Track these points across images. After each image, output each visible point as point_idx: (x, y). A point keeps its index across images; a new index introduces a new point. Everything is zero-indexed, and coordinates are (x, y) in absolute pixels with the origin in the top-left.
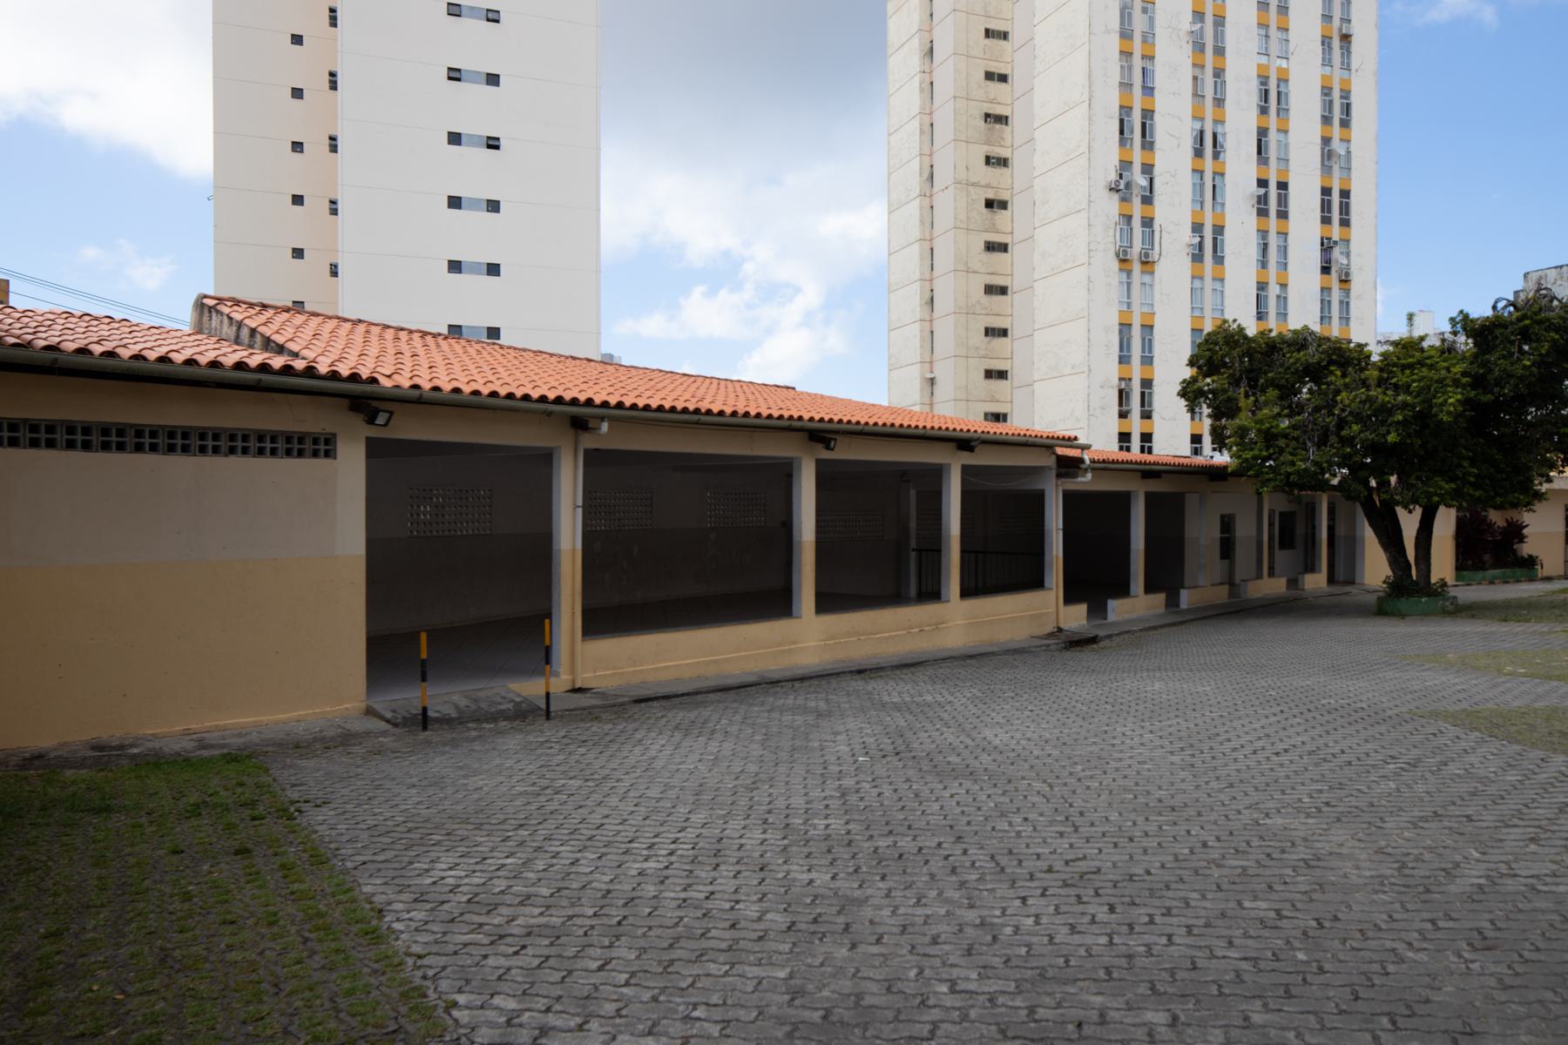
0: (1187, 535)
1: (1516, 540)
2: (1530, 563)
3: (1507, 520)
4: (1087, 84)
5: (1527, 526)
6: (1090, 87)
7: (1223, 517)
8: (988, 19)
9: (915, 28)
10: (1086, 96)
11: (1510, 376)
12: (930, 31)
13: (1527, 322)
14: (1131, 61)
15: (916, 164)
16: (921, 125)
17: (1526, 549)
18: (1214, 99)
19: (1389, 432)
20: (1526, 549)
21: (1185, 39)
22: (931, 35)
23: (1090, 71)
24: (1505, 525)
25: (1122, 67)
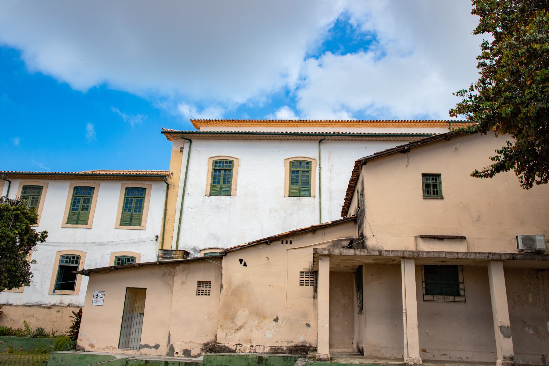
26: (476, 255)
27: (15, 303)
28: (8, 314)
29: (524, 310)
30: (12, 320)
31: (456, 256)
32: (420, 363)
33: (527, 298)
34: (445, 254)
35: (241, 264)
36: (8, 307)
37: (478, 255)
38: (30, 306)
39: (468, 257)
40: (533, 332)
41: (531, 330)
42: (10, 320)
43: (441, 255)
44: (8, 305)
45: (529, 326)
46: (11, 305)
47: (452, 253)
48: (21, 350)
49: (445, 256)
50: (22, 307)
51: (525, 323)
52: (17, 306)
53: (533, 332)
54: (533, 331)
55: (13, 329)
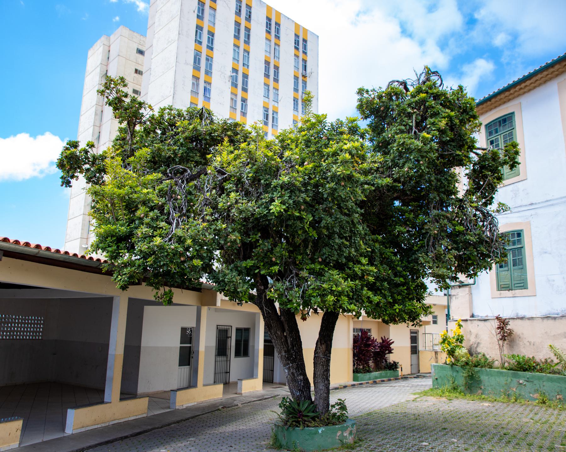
0: (143, 344)
1: (387, 352)
2: (394, 366)
3: (382, 338)
4: (173, 86)
5: (393, 342)
6: (174, 88)
7: (184, 330)
8: (137, 65)
9: (99, 62)
10: (172, 93)
11: (409, 150)
12: (107, 66)
13: (423, 95)
14: (198, 82)
15: (91, 130)
16: (96, 111)
17: (391, 358)
18: (241, 111)
19: (272, 200)
20: (391, 358)
21: (227, 79)
22: (107, 68)
23: (175, 80)
24: (381, 341)
25: (193, 84)
27: (528, 315)
28: (523, 334)
30: (532, 344)
36: (519, 322)
38: (555, 318)
42: (528, 344)
44: (518, 318)
46: (522, 318)
48: (559, 399)
50: (540, 320)
52: (531, 318)
55: (537, 359)
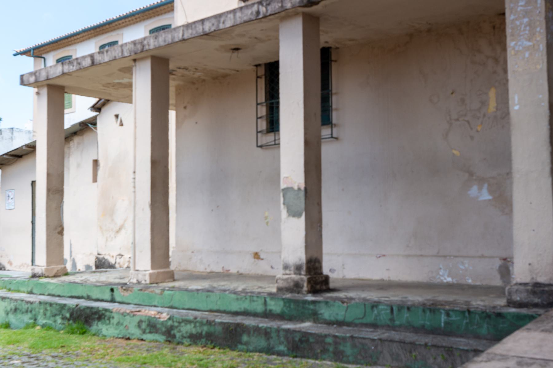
26: (234, 16)
29: (472, 138)
31: (200, 29)
32: (145, 281)
33: (484, 103)
34: (183, 31)
35: (117, 121)
37: (238, 14)
39: (221, 26)
40: (490, 197)
41: (485, 191)
43: (176, 35)
45: (481, 181)
47: (193, 26)
49: (183, 35)
51: (471, 174)
53: (490, 197)
54: (490, 192)
